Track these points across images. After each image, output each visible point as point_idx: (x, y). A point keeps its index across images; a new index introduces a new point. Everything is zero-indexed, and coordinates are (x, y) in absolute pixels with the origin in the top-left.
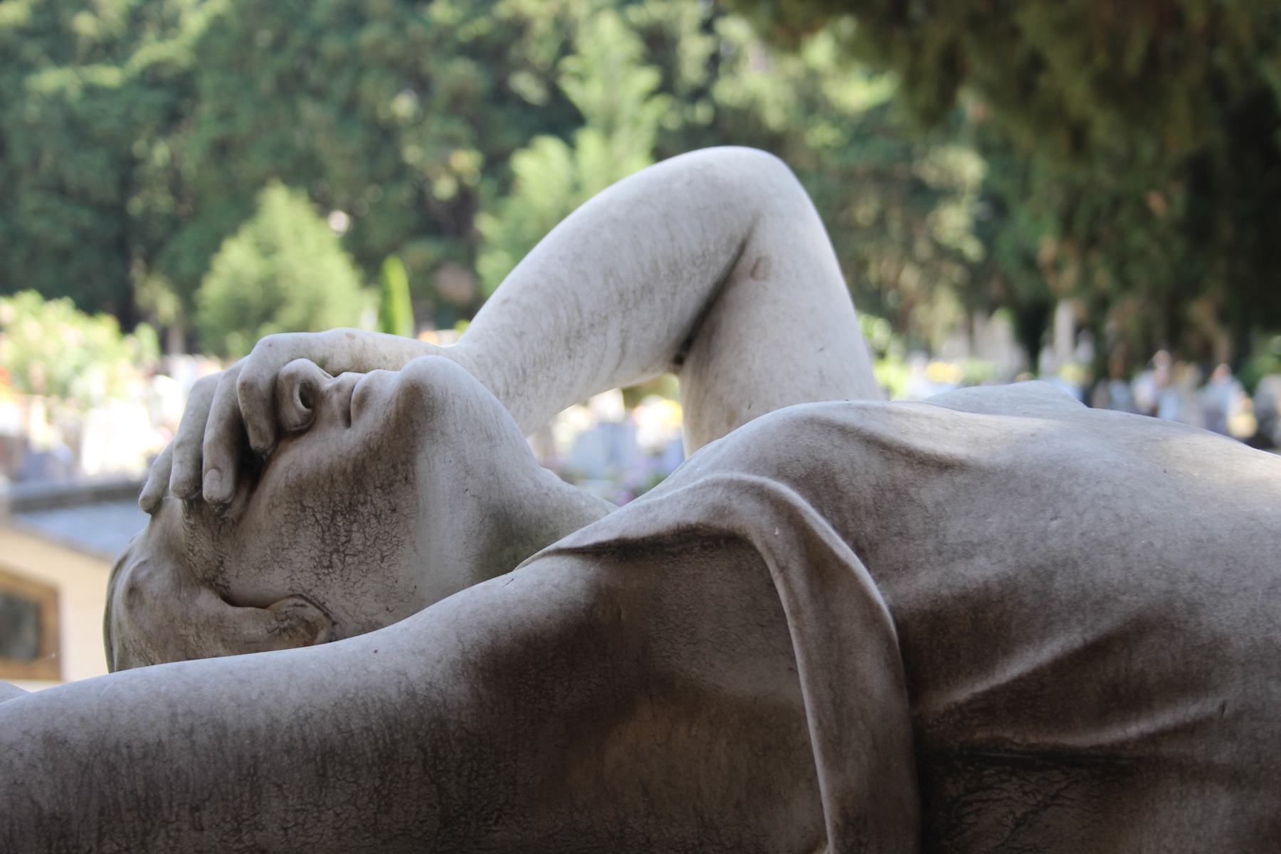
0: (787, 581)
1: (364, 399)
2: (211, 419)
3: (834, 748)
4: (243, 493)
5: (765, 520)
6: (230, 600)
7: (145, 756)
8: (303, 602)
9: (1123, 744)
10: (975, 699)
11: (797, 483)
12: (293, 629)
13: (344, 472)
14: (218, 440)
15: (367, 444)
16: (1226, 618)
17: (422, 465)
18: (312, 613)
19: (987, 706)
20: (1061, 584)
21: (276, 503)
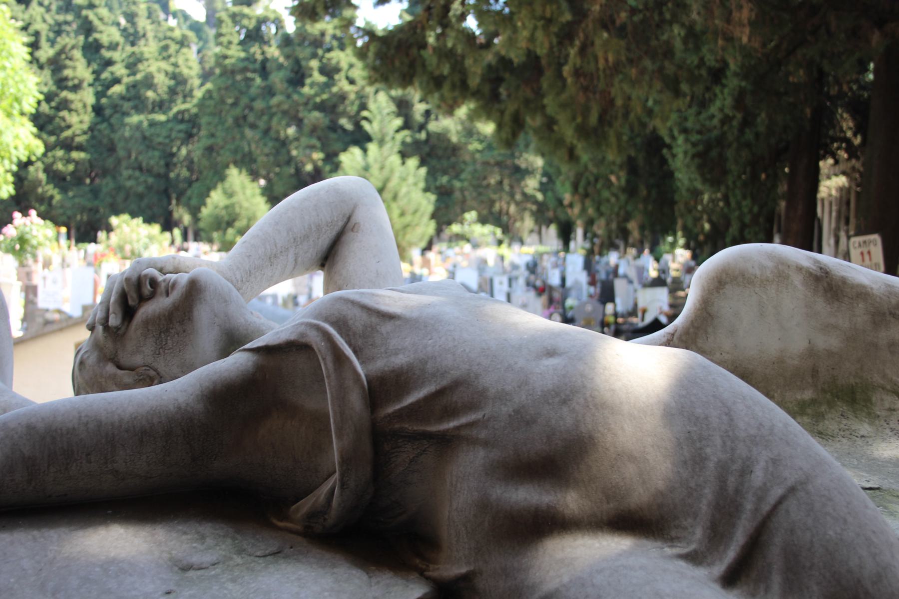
0: (325, 364)
1: (174, 285)
2: (114, 293)
4: (126, 324)
5: (318, 339)
6: (120, 367)
7: (68, 433)
9: (448, 430)
10: (395, 412)
11: (332, 324)
12: (144, 379)
13: (164, 316)
14: (116, 301)
15: (174, 304)
16: (489, 381)
17: (195, 313)
18: (152, 373)
19: (400, 415)
20: (430, 366)
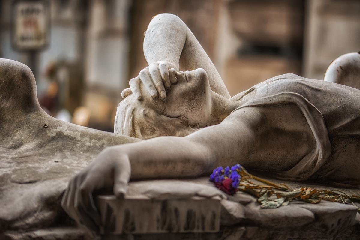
0: (306, 110)
1: (190, 77)
3: (320, 137)
8: (183, 117)
10: (338, 128)
11: (300, 93)
12: (183, 122)
18: (185, 119)
21: (178, 97)
